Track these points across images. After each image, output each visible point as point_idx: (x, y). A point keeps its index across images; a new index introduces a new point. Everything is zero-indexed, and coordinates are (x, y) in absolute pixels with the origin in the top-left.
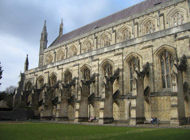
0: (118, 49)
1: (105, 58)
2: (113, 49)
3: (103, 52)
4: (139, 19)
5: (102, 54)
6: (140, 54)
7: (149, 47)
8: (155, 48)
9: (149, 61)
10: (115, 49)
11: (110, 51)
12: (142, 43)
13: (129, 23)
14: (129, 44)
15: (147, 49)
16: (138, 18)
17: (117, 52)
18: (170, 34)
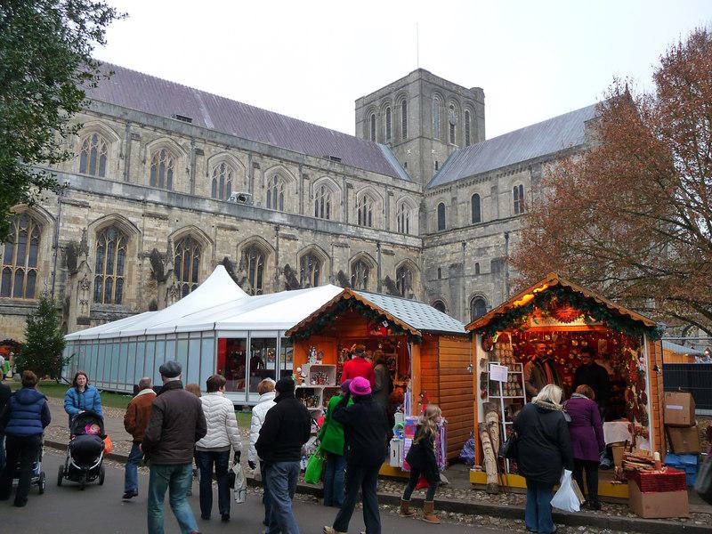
0: (156, 204)
1: (113, 211)
2: (142, 198)
3: (108, 192)
4: (144, 131)
5: (102, 195)
6: (208, 234)
7: (233, 229)
8: (240, 235)
9: (229, 255)
10: (148, 199)
11: (132, 200)
12: (216, 214)
13: (111, 123)
14: (186, 203)
15: (228, 232)
16: (143, 126)
17: (152, 209)
18: (270, 220)
